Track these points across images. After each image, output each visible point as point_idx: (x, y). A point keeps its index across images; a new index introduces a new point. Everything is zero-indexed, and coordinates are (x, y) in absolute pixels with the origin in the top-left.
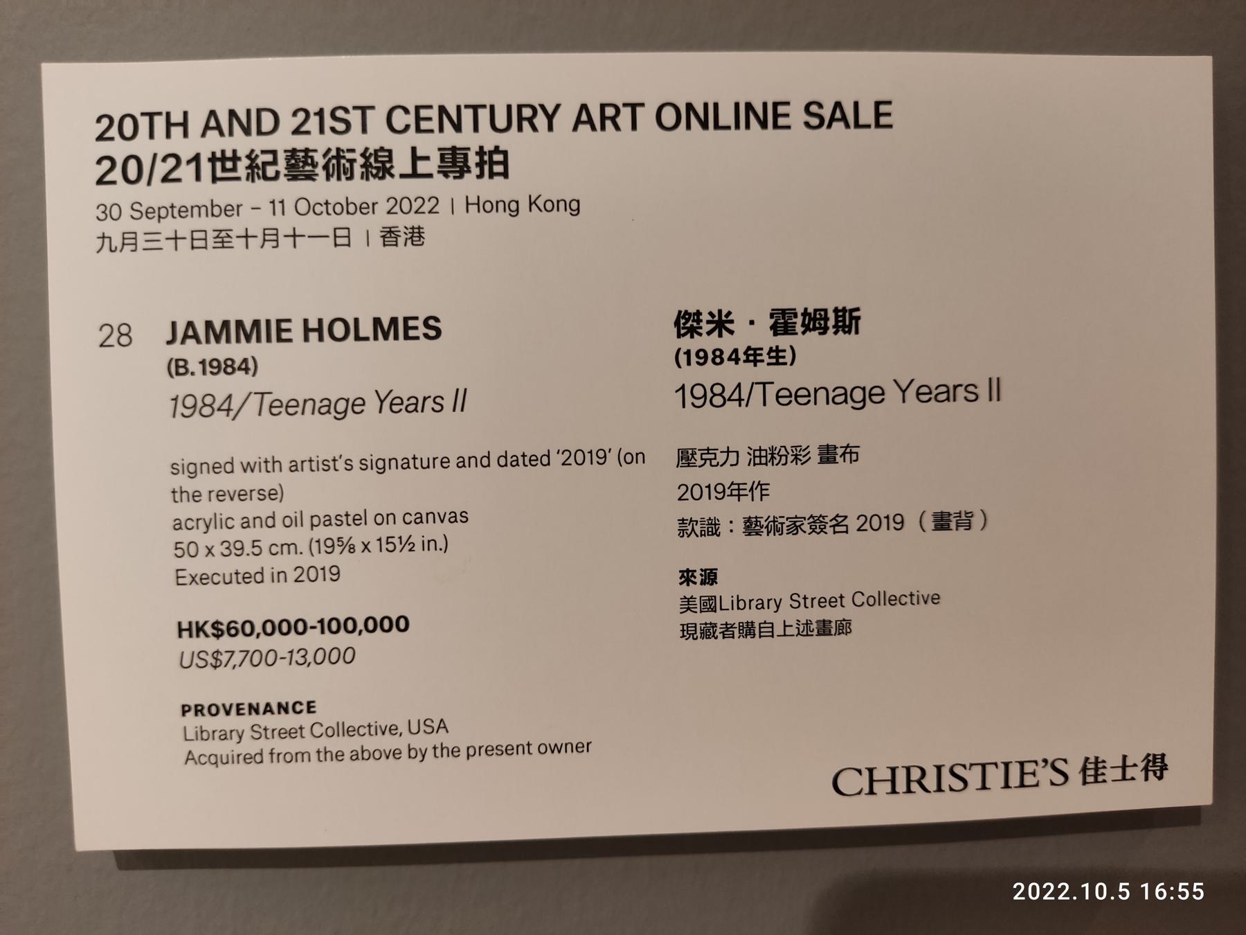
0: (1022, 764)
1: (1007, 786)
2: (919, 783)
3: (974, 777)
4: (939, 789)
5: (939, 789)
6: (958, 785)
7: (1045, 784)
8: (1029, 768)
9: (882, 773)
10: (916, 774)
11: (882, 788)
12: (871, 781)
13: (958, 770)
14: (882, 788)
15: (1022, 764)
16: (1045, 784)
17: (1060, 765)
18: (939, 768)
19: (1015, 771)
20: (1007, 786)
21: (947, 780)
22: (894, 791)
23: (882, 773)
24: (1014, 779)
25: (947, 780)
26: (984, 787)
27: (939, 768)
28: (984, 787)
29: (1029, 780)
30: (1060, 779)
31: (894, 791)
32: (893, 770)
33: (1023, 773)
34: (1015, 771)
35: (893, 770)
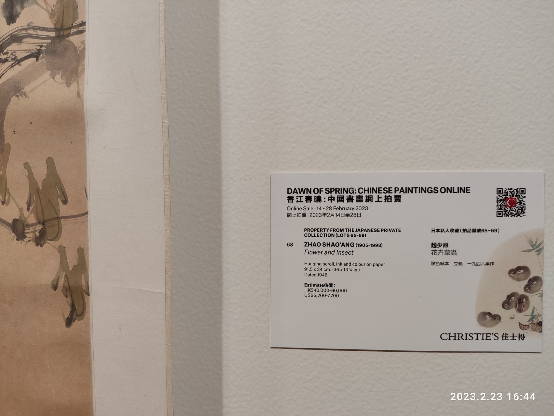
0: (487, 334)
1: (483, 339)
2: (461, 337)
3: (475, 337)
4: (466, 339)
5: (466, 339)
6: (471, 338)
7: (493, 339)
8: (488, 335)
9: (452, 335)
10: (461, 335)
11: (452, 338)
12: (450, 337)
13: (471, 335)
14: (452, 338)
15: (487, 334)
16: (493, 339)
17: (496, 335)
18: (466, 334)
19: (485, 336)
20: (483, 339)
21: (468, 337)
22: (455, 339)
23: (452, 335)
24: (485, 338)
25: (468, 337)
26: (477, 339)
27: (466, 334)
28: (477, 339)
29: (488, 338)
30: (496, 338)
31: (455, 339)
32: (455, 334)
33: (487, 336)
34: (485, 336)
35: (455, 334)
